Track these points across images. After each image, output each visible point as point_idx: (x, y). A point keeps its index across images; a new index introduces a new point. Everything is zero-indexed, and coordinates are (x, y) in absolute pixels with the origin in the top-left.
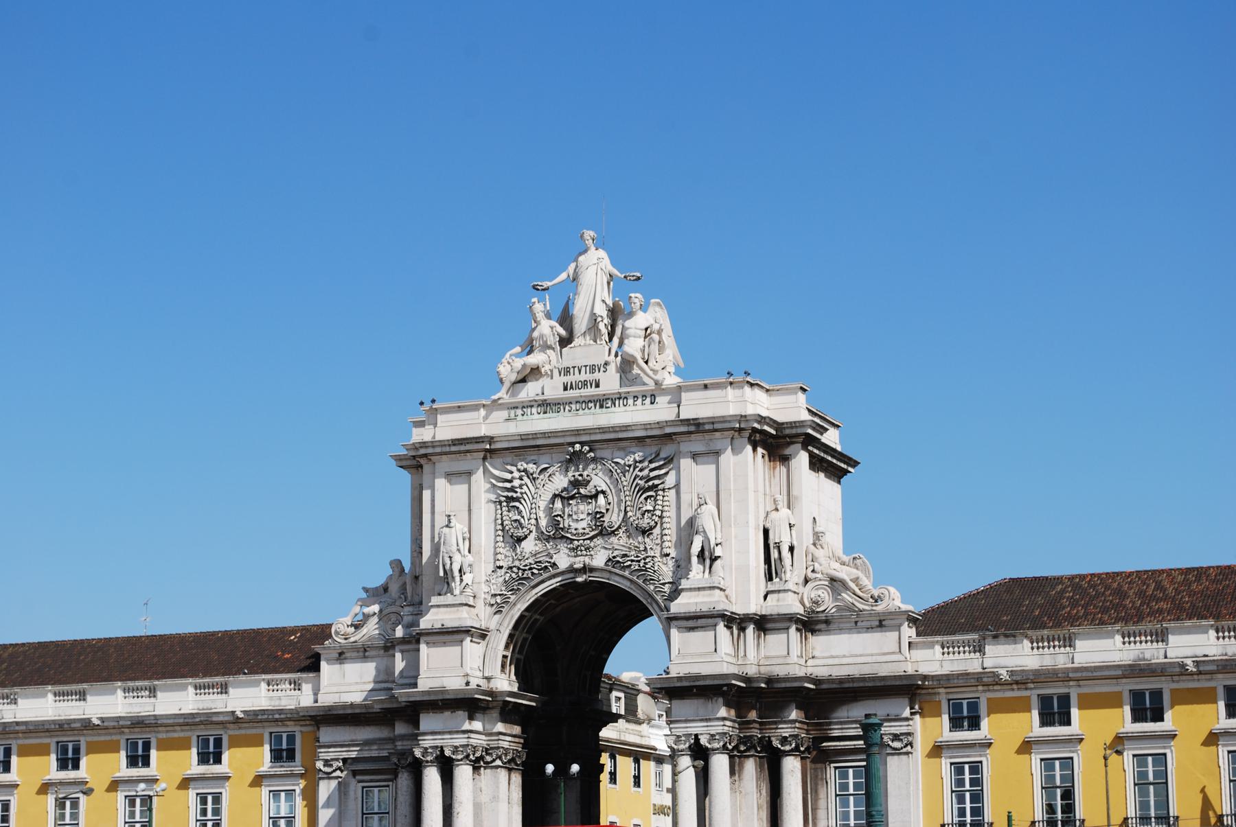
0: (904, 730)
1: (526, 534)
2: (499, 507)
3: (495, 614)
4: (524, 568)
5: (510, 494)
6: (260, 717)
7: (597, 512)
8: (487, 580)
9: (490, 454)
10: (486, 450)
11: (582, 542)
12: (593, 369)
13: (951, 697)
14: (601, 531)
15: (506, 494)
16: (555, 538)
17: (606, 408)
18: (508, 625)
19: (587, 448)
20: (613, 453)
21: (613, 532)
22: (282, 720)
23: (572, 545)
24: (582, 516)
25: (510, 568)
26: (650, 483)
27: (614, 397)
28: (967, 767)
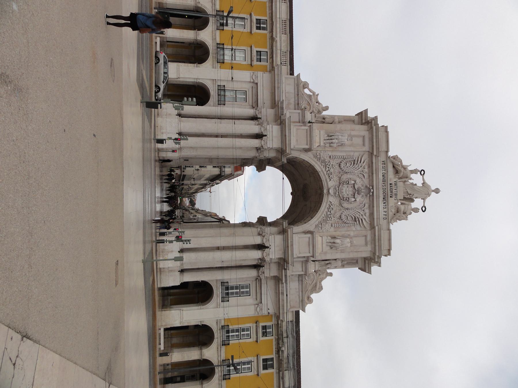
0: (264, 312)
4: (330, 167)
5: (356, 162)
6: (274, 48)
7: (349, 198)
9: (371, 154)
10: (372, 154)
11: (338, 191)
12: (396, 195)
13: (274, 326)
15: (356, 160)
16: (340, 180)
18: (308, 160)
19: (371, 194)
20: (368, 203)
22: (272, 57)
23: (336, 187)
24: (347, 192)
25: (330, 162)
26: (357, 220)
27: (387, 203)
28: (249, 332)
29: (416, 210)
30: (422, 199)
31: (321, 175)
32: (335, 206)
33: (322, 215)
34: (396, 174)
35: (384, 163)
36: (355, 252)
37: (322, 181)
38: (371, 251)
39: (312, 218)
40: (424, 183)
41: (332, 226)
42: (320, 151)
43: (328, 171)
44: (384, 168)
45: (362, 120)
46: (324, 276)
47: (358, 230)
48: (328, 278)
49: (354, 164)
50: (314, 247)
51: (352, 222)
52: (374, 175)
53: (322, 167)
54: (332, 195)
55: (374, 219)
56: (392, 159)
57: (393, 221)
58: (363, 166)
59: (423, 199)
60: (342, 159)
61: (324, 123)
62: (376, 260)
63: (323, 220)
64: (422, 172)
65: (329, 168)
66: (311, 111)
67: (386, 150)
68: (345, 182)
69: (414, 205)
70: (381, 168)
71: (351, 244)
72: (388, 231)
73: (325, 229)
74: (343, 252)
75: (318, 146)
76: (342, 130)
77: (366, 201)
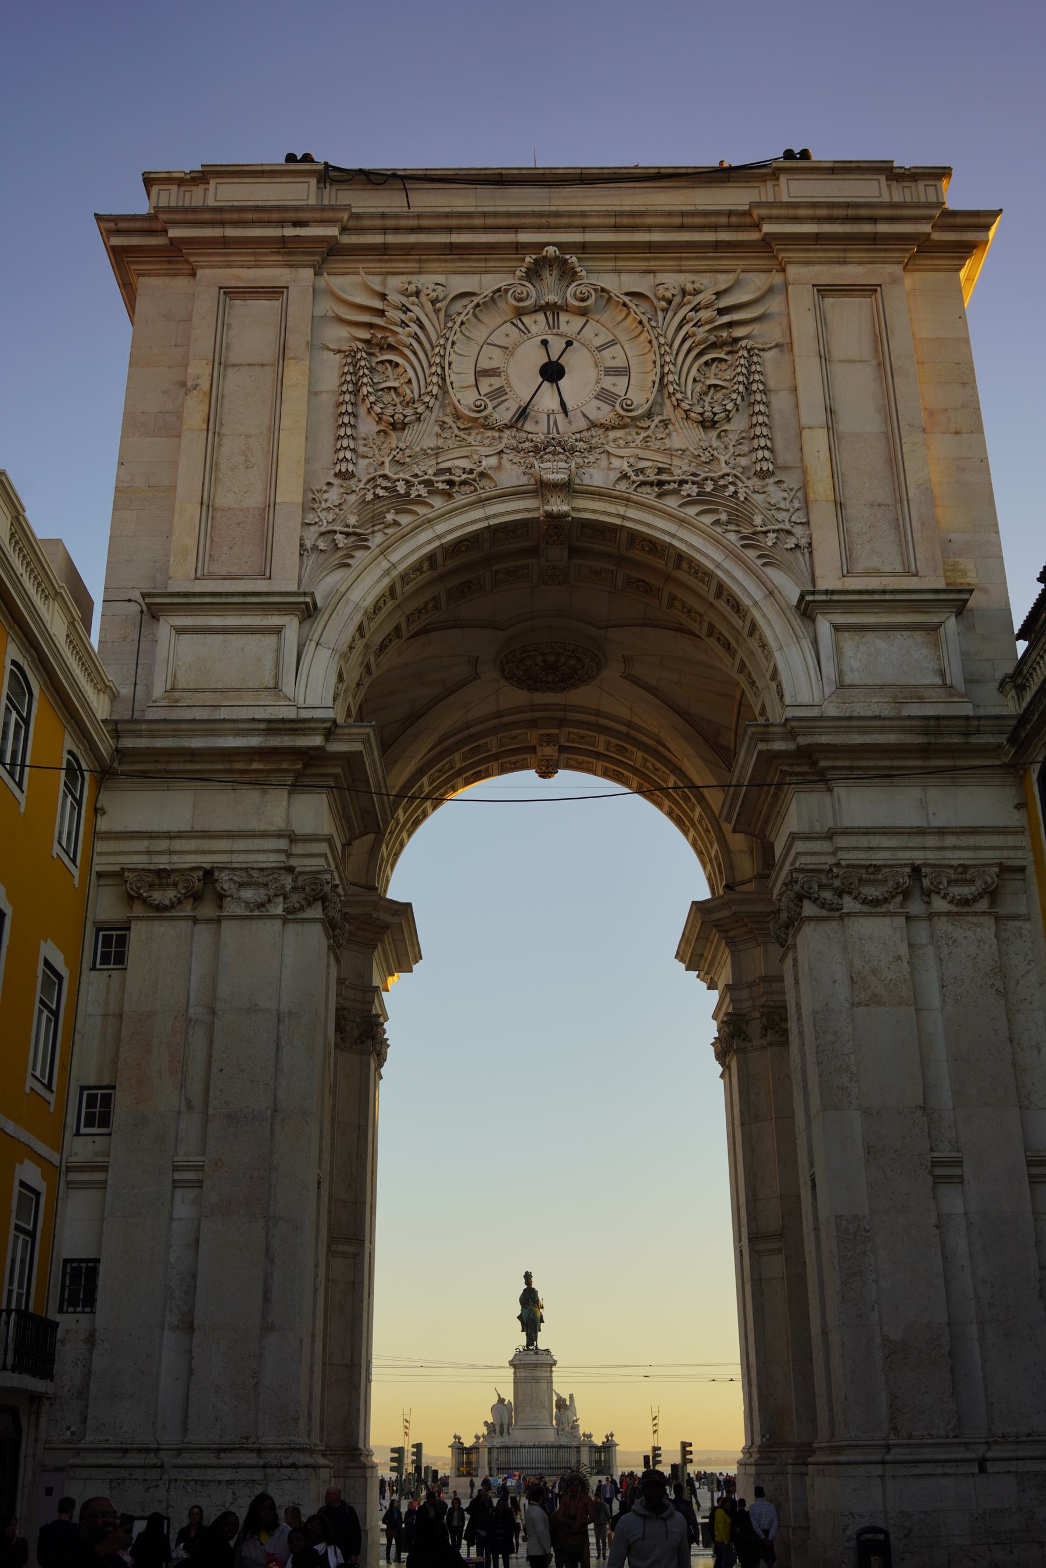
1: (419, 410)
26: (725, 334)
32: (641, 453)
37: (489, 527)
51: (742, 361)
58: (404, 300)
67: (313, 182)
72: (783, 179)
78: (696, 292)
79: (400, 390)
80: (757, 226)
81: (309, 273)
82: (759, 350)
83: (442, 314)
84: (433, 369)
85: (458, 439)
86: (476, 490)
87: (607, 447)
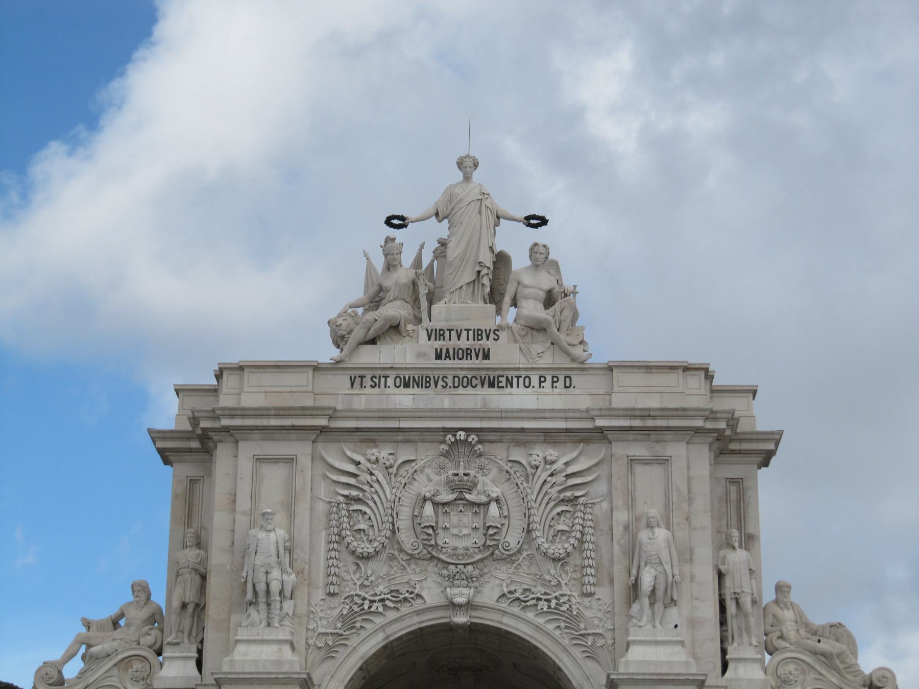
1: (377, 550)
2: (335, 509)
3: (323, 660)
4: (372, 598)
5: (354, 493)
7: (488, 527)
8: (312, 611)
10: (323, 430)
11: (463, 566)
12: (478, 334)
14: (492, 554)
15: (346, 492)
17: (498, 387)
19: (476, 439)
20: (508, 451)
21: (510, 556)
23: (445, 572)
24: (465, 531)
25: (352, 596)
26: (568, 494)
27: (510, 374)
29: (538, 256)
30: (497, 224)
31: (399, 630)
32: (515, 578)
33: (547, 633)
34: (399, 333)
35: (357, 380)
36: (690, 505)
38: (687, 443)
39: (560, 669)
40: (437, 214)
41: (591, 595)
42: (310, 633)
43: (385, 606)
44: (376, 380)
45: (190, 450)
46: (788, 615)
47: (610, 492)
48: (794, 596)
49: (358, 500)
50: (665, 677)
51: (579, 514)
52: (404, 424)
53: (368, 626)
54: (477, 592)
55: (567, 430)
56: (346, 348)
57: (577, 351)
58: (369, 465)
59: (498, 218)
60: (342, 548)
61: (200, 608)
62: (722, 425)
63: (566, 627)
64: (396, 222)
65: (375, 601)
66: (150, 654)
68: (426, 539)
69: (520, 261)
70: (376, 390)
71: (658, 526)
72: (615, 371)
73: (601, 620)
74: (691, 555)
75: (293, 648)
76: (233, 543)
77: (499, 453)
78: (552, 463)
79: (366, 532)
80: (592, 419)
81: (307, 447)
82: (591, 504)
83: (393, 476)
84: (387, 518)
85: (402, 567)
86: (412, 605)
87: (494, 574)
